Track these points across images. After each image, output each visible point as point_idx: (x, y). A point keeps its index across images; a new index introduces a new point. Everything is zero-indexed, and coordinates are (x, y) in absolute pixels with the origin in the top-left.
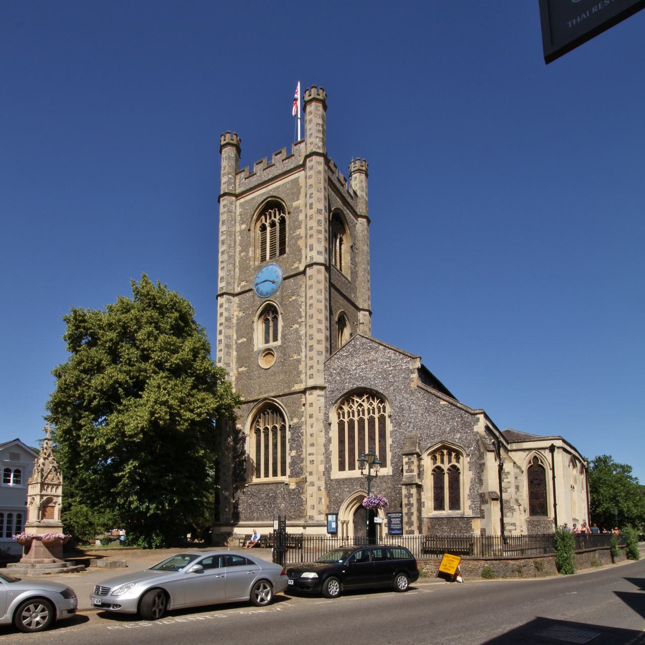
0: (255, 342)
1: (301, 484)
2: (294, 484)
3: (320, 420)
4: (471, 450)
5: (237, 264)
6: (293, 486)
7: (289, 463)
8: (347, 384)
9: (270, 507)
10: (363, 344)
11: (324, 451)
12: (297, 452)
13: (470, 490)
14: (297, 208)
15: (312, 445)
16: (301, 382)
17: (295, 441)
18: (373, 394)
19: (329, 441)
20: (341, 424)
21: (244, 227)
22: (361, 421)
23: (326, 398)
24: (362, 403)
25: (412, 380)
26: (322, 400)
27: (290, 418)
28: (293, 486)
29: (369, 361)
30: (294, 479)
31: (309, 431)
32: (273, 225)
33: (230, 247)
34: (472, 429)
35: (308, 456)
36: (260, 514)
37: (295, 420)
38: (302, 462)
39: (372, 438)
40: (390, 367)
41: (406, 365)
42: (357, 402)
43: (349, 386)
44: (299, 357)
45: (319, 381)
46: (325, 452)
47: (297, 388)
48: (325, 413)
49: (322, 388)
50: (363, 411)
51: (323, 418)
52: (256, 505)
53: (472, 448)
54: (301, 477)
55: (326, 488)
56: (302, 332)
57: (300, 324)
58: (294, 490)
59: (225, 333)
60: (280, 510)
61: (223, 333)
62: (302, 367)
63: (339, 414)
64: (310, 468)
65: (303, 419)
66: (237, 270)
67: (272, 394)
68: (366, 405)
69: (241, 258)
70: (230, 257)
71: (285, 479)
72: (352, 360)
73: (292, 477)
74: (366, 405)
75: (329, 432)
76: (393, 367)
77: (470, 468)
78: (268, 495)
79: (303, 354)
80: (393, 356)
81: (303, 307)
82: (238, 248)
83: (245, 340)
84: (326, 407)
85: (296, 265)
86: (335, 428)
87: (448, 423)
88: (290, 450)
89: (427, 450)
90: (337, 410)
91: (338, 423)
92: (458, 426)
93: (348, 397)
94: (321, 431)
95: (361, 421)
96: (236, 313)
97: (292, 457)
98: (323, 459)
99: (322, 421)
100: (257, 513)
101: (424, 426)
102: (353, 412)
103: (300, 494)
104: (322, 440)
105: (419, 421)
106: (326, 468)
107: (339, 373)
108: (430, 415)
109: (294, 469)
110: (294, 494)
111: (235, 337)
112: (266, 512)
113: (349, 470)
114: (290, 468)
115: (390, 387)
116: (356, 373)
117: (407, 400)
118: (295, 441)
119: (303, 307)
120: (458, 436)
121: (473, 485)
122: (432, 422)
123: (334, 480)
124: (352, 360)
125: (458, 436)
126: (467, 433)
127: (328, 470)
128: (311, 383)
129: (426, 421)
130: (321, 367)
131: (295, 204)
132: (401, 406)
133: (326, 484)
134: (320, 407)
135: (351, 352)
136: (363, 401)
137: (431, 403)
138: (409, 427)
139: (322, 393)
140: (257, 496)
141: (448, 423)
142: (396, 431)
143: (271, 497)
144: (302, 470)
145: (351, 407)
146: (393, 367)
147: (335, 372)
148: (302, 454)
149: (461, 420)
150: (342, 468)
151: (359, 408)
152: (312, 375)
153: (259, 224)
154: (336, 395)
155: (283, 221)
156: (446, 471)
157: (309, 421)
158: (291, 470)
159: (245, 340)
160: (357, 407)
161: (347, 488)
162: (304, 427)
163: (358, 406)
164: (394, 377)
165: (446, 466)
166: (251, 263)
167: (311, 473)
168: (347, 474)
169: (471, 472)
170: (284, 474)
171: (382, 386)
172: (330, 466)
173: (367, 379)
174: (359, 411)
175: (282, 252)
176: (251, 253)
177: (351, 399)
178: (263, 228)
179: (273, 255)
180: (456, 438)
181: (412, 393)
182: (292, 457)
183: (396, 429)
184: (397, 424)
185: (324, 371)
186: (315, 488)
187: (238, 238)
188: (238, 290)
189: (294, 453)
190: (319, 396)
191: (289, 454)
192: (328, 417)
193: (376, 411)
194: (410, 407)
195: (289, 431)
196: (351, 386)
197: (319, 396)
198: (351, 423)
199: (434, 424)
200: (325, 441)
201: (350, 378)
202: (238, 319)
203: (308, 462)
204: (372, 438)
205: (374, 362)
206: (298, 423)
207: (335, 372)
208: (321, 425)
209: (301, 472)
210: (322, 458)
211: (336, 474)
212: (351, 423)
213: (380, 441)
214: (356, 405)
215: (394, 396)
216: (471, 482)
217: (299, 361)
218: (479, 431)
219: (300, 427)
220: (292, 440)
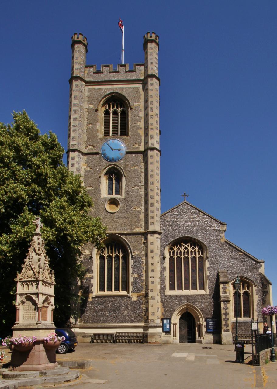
3: (158, 254)
4: (257, 283)
6: (134, 299)
7: (132, 282)
8: (177, 233)
9: (114, 313)
10: (189, 209)
12: (138, 275)
13: (257, 306)
15: (153, 271)
17: (137, 267)
18: (194, 242)
19: (164, 269)
20: (172, 259)
22: (186, 259)
23: (161, 240)
24: (187, 247)
25: (221, 237)
26: (159, 240)
28: (134, 299)
29: (193, 221)
30: (135, 294)
34: (258, 271)
35: (149, 278)
36: (106, 319)
39: (194, 270)
40: (207, 227)
41: (218, 228)
43: (178, 235)
46: (161, 277)
48: (161, 251)
49: (159, 233)
50: (188, 252)
51: (159, 253)
52: (102, 312)
53: (258, 282)
54: (142, 293)
60: (124, 316)
63: (170, 252)
72: (181, 218)
73: (134, 292)
74: (190, 249)
75: (164, 264)
76: (209, 227)
77: (257, 293)
78: (113, 304)
80: (209, 221)
84: (161, 246)
87: (244, 266)
88: (133, 273)
89: (231, 281)
90: (169, 250)
91: (169, 258)
92: (250, 268)
94: (159, 262)
95: (186, 259)
97: (134, 278)
98: (160, 281)
99: (159, 255)
100: (103, 317)
101: (229, 266)
102: (181, 252)
103: (141, 304)
105: (226, 263)
106: (161, 288)
107: (171, 225)
108: (233, 260)
109: (136, 287)
110: (136, 304)
112: (111, 316)
115: (207, 239)
116: (184, 227)
117: (219, 249)
118: (137, 267)
120: (250, 274)
121: (259, 303)
122: (234, 264)
123: (168, 296)
124: (181, 218)
125: (250, 274)
126: (255, 273)
127: (163, 289)
129: (230, 263)
130: (158, 219)
132: (215, 252)
134: (158, 246)
135: (180, 213)
136: (188, 246)
137: (233, 253)
138: (220, 265)
139: (159, 236)
140: (103, 305)
141: (244, 266)
142: (211, 267)
143: (116, 306)
145: (179, 249)
146: (209, 227)
147: (168, 224)
148: (142, 277)
149: (252, 265)
150: (172, 288)
151: (185, 250)
152: (153, 223)
154: (169, 239)
156: (242, 294)
158: (134, 287)
160: (184, 249)
164: (210, 233)
165: (242, 291)
169: (257, 296)
170: (126, 288)
171: (202, 238)
172: (165, 287)
180: (249, 275)
181: (222, 245)
182: (134, 278)
183: (211, 266)
184: (212, 263)
185: (160, 222)
189: (136, 275)
190: (157, 238)
191: (132, 276)
192: (164, 253)
194: (220, 253)
196: (180, 235)
197: (157, 238)
198: (179, 259)
199: (236, 266)
204: (194, 270)
205: (196, 222)
207: (168, 224)
209: (142, 289)
211: (169, 292)
212: (179, 259)
213: (199, 273)
214: (183, 248)
215: (210, 245)
216: (258, 301)
218: (262, 272)
219: (141, 257)
220: (135, 266)
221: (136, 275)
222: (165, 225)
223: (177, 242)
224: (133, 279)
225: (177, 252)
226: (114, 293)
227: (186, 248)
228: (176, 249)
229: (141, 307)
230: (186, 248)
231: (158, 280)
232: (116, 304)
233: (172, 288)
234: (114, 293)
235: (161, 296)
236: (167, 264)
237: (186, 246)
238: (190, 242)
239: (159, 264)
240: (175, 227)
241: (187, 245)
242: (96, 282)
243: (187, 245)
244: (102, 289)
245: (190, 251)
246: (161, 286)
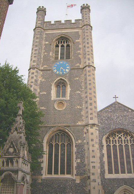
0: (52, 95)
1: (86, 179)
2: (79, 180)
5: (42, 57)
6: (78, 181)
11: (99, 161)
14: (78, 42)
15: (94, 157)
16: (83, 120)
19: (103, 155)
20: (108, 147)
21: (47, 43)
22: (121, 146)
23: (99, 131)
27: (76, 140)
28: (78, 181)
30: (79, 177)
31: (91, 148)
32: (62, 46)
33: (39, 49)
35: (91, 163)
37: (80, 141)
38: (85, 167)
42: (118, 136)
43: (113, 127)
44: (81, 107)
45: (95, 121)
47: (80, 124)
48: (99, 140)
50: (121, 141)
55: (102, 184)
56: (83, 95)
57: (81, 91)
58: (78, 184)
59: (34, 87)
61: (33, 87)
62: (83, 113)
63: (107, 141)
64: (92, 171)
65: (85, 141)
66: (42, 60)
67: (64, 125)
68: (123, 138)
69: (45, 56)
70: (39, 53)
71: (74, 178)
74: (123, 138)
79: (84, 106)
81: (83, 84)
82: (43, 51)
83: (46, 93)
84: (99, 136)
86: (105, 148)
88: (76, 158)
90: (106, 139)
91: (106, 146)
93: (113, 134)
95: (121, 146)
96: (40, 79)
99: (98, 143)
104: (98, 155)
106: (101, 172)
110: (79, 187)
111: (39, 90)
113: (115, 174)
114: (76, 170)
119: (83, 84)
127: (103, 173)
133: (101, 181)
139: (98, 128)
143: (62, 187)
144: (84, 171)
150: (110, 172)
155: (68, 46)
157: (91, 143)
159: (46, 93)
161: (116, 184)
162: (86, 146)
163: (119, 138)
166: (51, 58)
167: (93, 174)
168: (114, 176)
172: (104, 171)
173: (123, 125)
174: (119, 141)
175: (68, 57)
176: (51, 54)
177: (114, 133)
179: (62, 58)
182: (77, 163)
186: (96, 183)
190: (96, 129)
191: (76, 161)
192: (102, 142)
193: (129, 142)
195: (76, 147)
196: (115, 127)
197: (96, 129)
198: (115, 146)
200: (100, 156)
201: (113, 123)
202: (41, 82)
203: (91, 167)
206: (81, 143)
208: (97, 146)
210: (99, 165)
211: (108, 176)
212: (115, 146)
217: (81, 110)
220: (77, 153)
221: (79, 161)
222: (102, 120)
223: (113, 134)
224: (77, 164)
225: (113, 141)
226: (60, 176)
227: (120, 138)
228: (111, 139)
229: (84, 189)
230: (120, 138)
231: (98, 165)
232: (61, 186)
233: (110, 172)
234: (60, 176)
235: (101, 179)
236: (105, 151)
237: (120, 136)
238: (123, 132)
239: (99, 151)
240: (110, 121)
241: (120, 135)
242: (45, 165)
243: (120, 135)
244: (50, 172)
245: (123, 140)
246: (101, 170)
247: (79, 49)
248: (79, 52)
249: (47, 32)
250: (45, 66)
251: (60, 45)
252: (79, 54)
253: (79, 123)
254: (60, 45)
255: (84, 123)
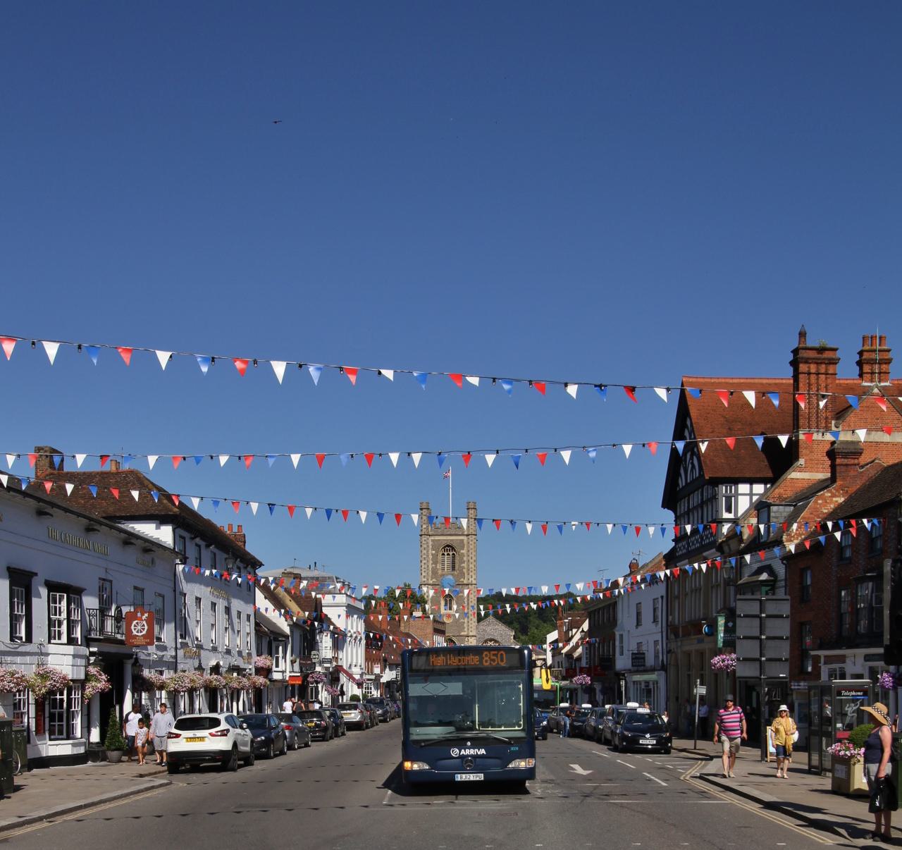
14: (463, 553)
21: (434, 552)
62: (465, 625)
69: (433, 568)
82: (431, 562)
85: (462, 580)
128: (471, 634)
131: (462, 551)
153: (441, 553)
178: (443, 554)
187: (431, 557)
188: (431, 582)
247: (464, 562)
248: (463, 565)
249: (433, 538)
250: (434, 580)
251: (446, 553)
252: (463, 567)
253: (462, 633)
254: (446, 553)
255: (465, 633)
